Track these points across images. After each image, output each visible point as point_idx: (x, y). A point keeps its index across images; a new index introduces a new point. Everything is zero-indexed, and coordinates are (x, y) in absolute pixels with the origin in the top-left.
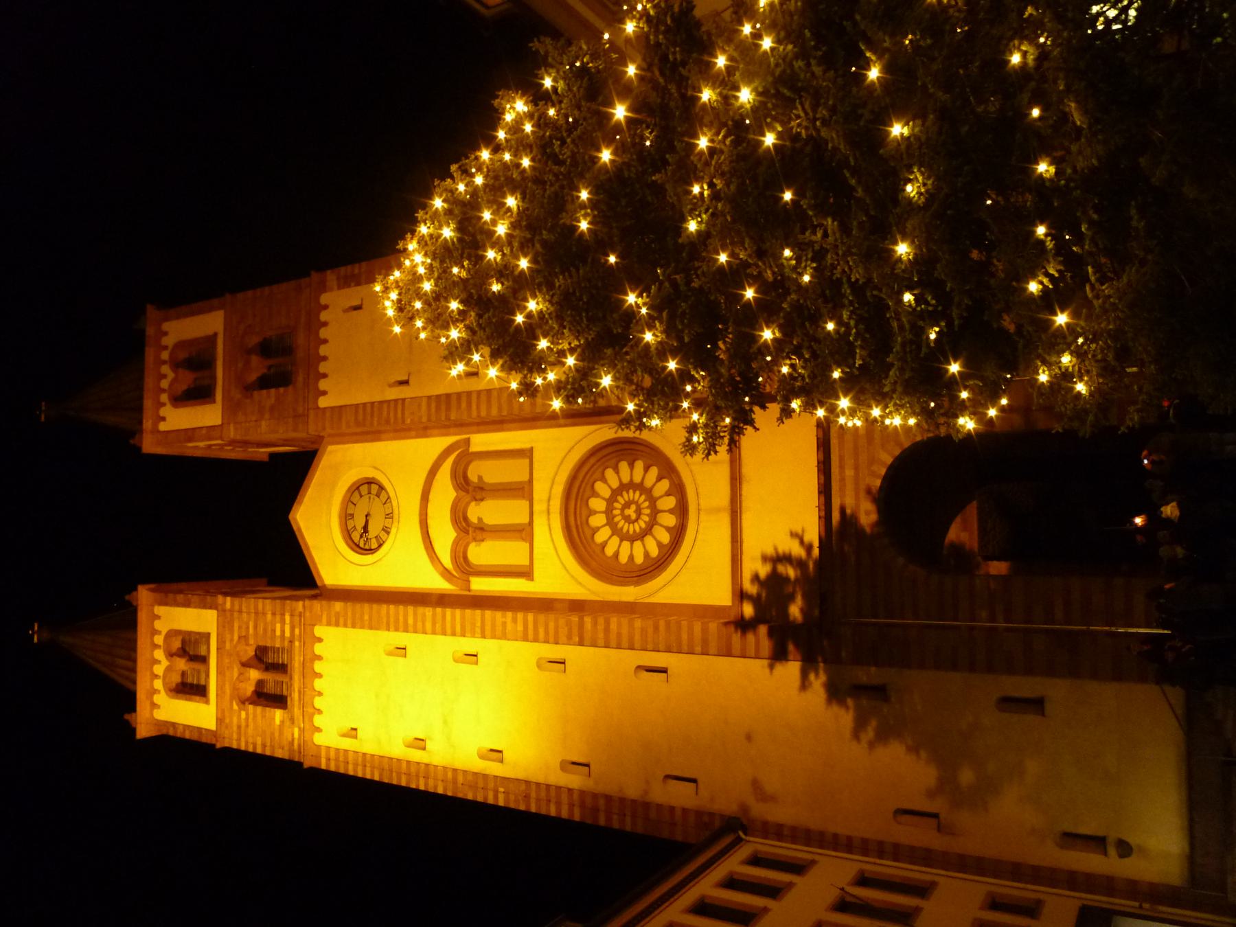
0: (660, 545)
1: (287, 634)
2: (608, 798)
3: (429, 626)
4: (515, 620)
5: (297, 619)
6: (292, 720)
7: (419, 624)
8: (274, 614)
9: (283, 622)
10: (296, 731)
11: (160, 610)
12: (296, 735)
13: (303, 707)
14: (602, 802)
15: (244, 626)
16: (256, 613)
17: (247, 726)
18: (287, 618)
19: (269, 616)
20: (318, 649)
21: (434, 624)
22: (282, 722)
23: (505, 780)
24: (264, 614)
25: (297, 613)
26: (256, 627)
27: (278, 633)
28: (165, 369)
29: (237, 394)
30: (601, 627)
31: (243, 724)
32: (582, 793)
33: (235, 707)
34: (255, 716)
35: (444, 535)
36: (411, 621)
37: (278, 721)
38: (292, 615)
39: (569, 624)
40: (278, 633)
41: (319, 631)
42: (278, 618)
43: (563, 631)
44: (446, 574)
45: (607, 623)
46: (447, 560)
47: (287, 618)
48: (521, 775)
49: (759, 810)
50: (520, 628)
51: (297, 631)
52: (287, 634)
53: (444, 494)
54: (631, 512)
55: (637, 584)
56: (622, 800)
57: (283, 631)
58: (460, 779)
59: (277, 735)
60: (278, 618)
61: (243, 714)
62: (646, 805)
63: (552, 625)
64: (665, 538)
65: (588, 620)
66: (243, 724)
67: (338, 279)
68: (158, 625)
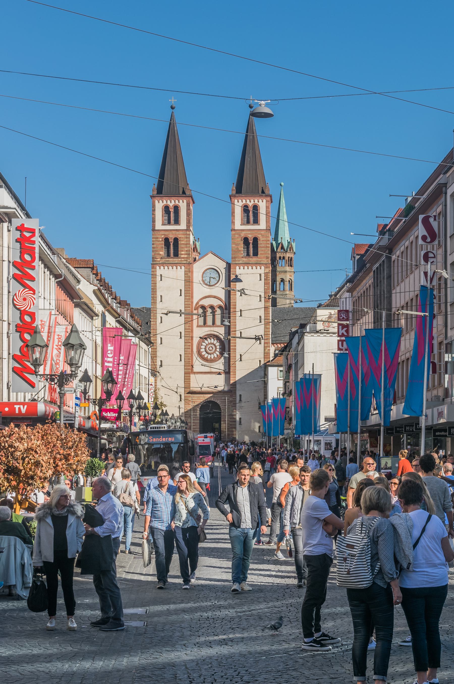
0: (204, 355)
1: (182, 256)
2: (156, 349)
3: (186, 303)
4: (189, 326)
5: (185, 259)
6: (161, 258)
7: (186, 300)
8: (187, 251)
9: (185, 254)
10: (159, 260)
11: (185, 201)
12: (158, 260)
13: (166, 264)
14: (155, 347)
15: (183, 239)
16: (186, 244)
17: (158, 241)
18: (186, 256)
19: (186, 249)
20: (179, 267)
21: (187, 304)
22: (160, 255)
23: (156, 324)
24: (186, 247)
25: (187, 259)
26: (183, 244)
27: (182, 253)
28: (252, 202)
29: (243, 235)
30: (188, 347)
31: (159, 240)
32: (156, 343)
33: (163, 236)
34: (162, 244)
35: (206, 302)
36: (187, 298)
37: (161, 253)
38: (187, 258)
39: (189, 340)
40: (182, 253)
41: (183, 267)
42: (186, 252)
43: (187, 338)
44: (197, 303)
45: (189, 348)
46: (201, 303)
47: (186, 256)
48: (158, 328)
49: (159, 379)
50: (187, 328)
51: (183, 260)
52: (182, 256)
53: (216, 303)
54: (211, 348)
55: (197, 352)
56: (156, 352)
57: (182, 254)
58: (155, 312)
59: (157, 253)
60: (186, 252)
61: (161, 240)
62: (156, 357)
63: (188, 336)
64: (206, 356)
65: (190, 344)
66: (159, 240)
67: (267, 273)
68: (181, 201)
